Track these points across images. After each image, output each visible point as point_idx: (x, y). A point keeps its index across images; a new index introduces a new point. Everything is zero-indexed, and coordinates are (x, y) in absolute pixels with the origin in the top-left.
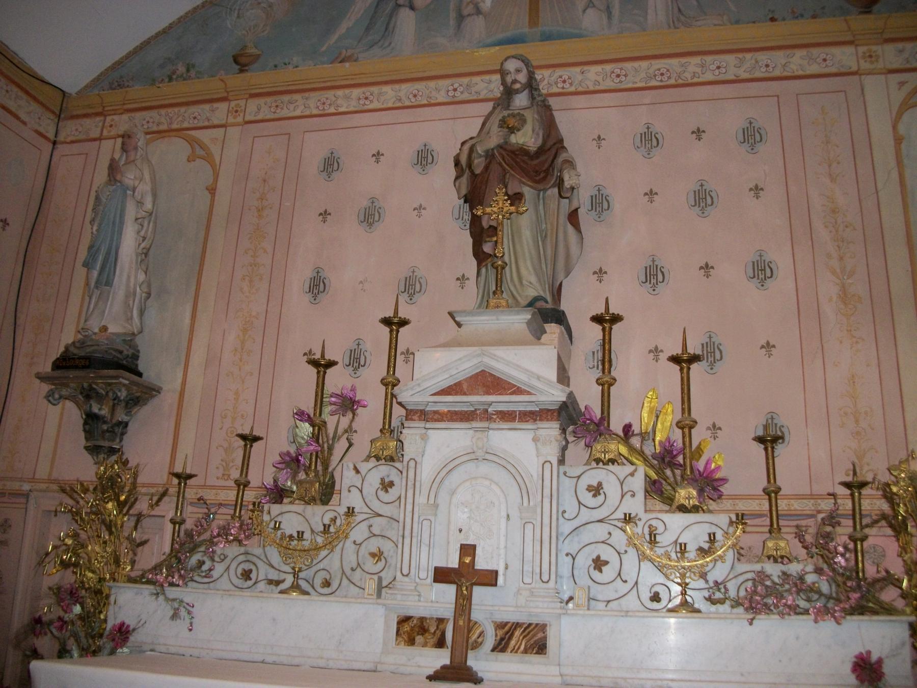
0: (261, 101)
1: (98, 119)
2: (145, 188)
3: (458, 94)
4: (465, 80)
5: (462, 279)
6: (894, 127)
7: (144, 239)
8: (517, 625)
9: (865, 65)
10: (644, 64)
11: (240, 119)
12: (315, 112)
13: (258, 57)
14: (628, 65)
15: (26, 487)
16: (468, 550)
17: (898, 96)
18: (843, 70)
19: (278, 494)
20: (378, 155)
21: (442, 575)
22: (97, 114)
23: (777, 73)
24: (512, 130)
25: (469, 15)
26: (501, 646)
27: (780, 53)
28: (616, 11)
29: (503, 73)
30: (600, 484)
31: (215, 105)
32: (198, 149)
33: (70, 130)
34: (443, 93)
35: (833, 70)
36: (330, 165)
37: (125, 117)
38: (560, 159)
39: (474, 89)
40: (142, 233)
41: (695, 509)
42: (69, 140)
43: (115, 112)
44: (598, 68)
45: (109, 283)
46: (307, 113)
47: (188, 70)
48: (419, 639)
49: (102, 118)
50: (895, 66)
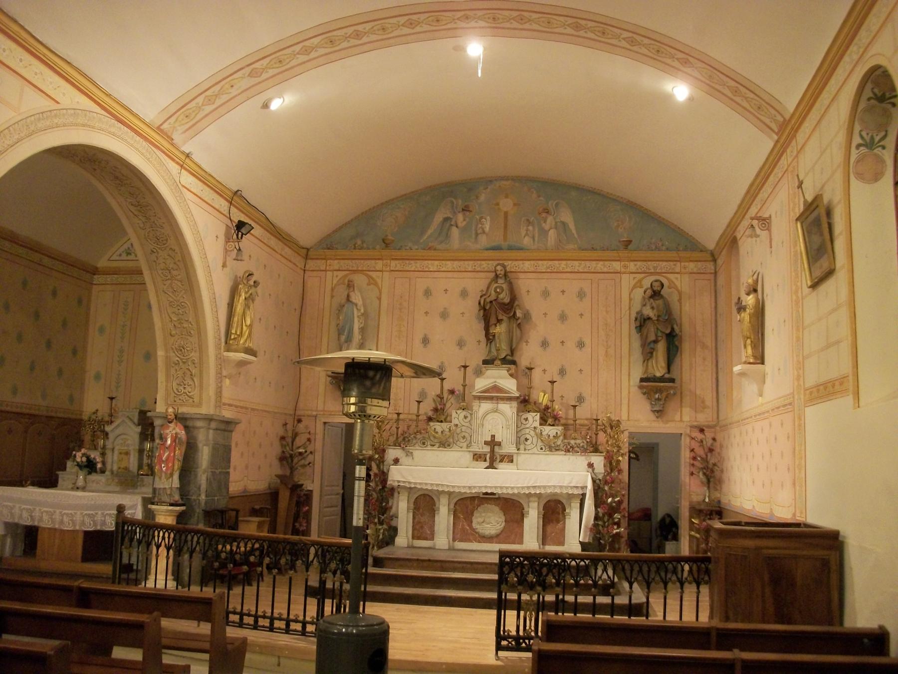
0: (397, 262)
1: (323, 261)
2: (360, 303)
3: (476, 268)
4: (479, 262)
5: (479, 342)
6: (630, 295)
7: (361, 323)
8: (506, 456)
9: (623, 270)
10: (545, 262)
11: (388, 269)
12: (420, 270)
13: (393, 241)
14: (540, 262)
15: (314, 413)
16: (493, 436)
17: (633, 283)
18: (616, 271)
19: (430, 419)
20: (446, 290)
21: (486, 443)
22: (324, 259)
23: (592, 270)
24: (499, 293)
25: (481, 233)
26: (501, 461)
27: (594, 262)
28: (536, 239)
29: (496, 271)
30: (527, 418)
31: (377, 261)
32: (371, 280)
33: (311, 264)
34: (470, 267)
35: (612, 271)
36: (428, 293)
37: (336, 261)
38: (515, 305)
39: (482, 267)
40: (361, 321)
41: (553, 425)
42: (311, 269)
43: (331, 259)
44: (529, 262)
45: (351, 341)
46: (416, 270)
47: (362, 243)
48: (479, 460)
49: (325, 261)
50: (634, 271)
